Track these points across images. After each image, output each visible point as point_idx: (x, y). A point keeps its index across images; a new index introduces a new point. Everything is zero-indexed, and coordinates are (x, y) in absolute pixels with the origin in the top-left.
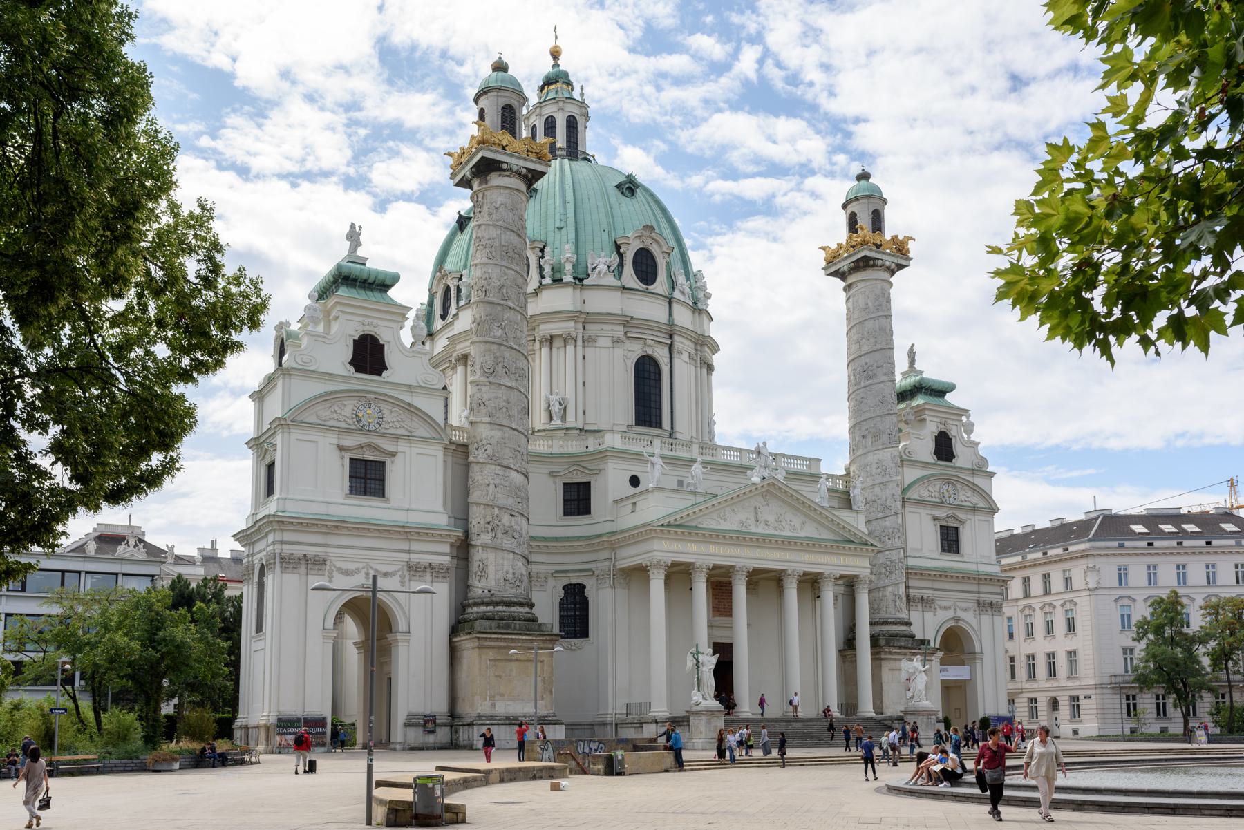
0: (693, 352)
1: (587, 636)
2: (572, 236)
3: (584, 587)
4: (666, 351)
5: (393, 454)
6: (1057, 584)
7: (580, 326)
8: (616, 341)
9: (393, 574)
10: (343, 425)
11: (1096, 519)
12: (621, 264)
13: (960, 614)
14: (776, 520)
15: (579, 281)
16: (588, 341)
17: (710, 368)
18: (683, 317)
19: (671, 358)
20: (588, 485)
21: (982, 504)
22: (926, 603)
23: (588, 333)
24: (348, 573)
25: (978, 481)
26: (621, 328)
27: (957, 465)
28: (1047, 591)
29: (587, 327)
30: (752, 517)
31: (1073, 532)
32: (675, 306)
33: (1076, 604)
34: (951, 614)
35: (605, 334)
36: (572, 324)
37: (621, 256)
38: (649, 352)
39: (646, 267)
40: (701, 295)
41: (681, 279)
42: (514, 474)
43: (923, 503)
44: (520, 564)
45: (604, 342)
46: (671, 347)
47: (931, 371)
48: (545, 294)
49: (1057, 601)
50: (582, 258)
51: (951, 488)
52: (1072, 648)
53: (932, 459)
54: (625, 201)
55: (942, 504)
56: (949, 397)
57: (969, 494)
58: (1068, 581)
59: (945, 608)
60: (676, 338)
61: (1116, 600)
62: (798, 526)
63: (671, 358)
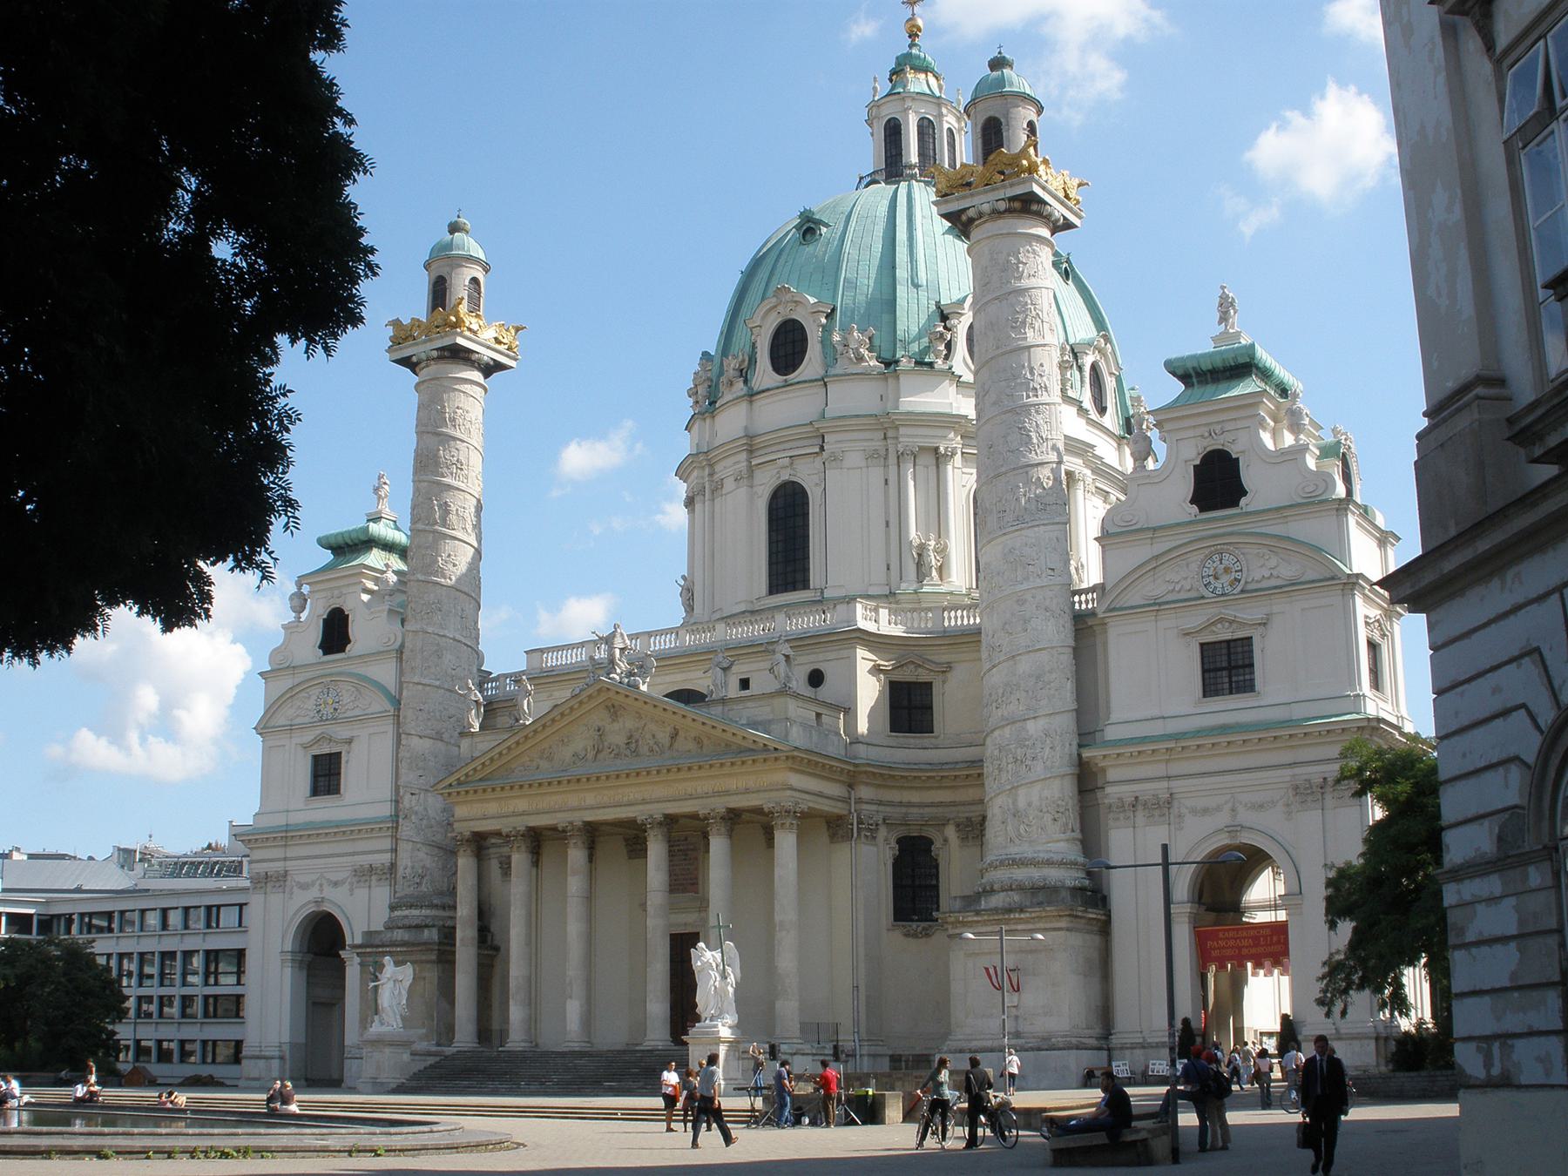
0: (878, 444)
5: (350, 741)
9: (343, 882)
10: (306, 720)
12: (752, 360)
13: (1245, 817)
16: (717, 488)
22: (1163, 807)
24: (304, 887)
26: (744, 456)
27: (1250, 509)
29: (718, 468)
34: (1223, 819)
36: (695, 473)
37: (754, 346)
38: (785, 477)
39: (788, 346)
42: (415, 741)
43: (1157, 606)
44: (421, 855)
45: (729, 484)
57: (1273, 562)
59: (1205, 811)
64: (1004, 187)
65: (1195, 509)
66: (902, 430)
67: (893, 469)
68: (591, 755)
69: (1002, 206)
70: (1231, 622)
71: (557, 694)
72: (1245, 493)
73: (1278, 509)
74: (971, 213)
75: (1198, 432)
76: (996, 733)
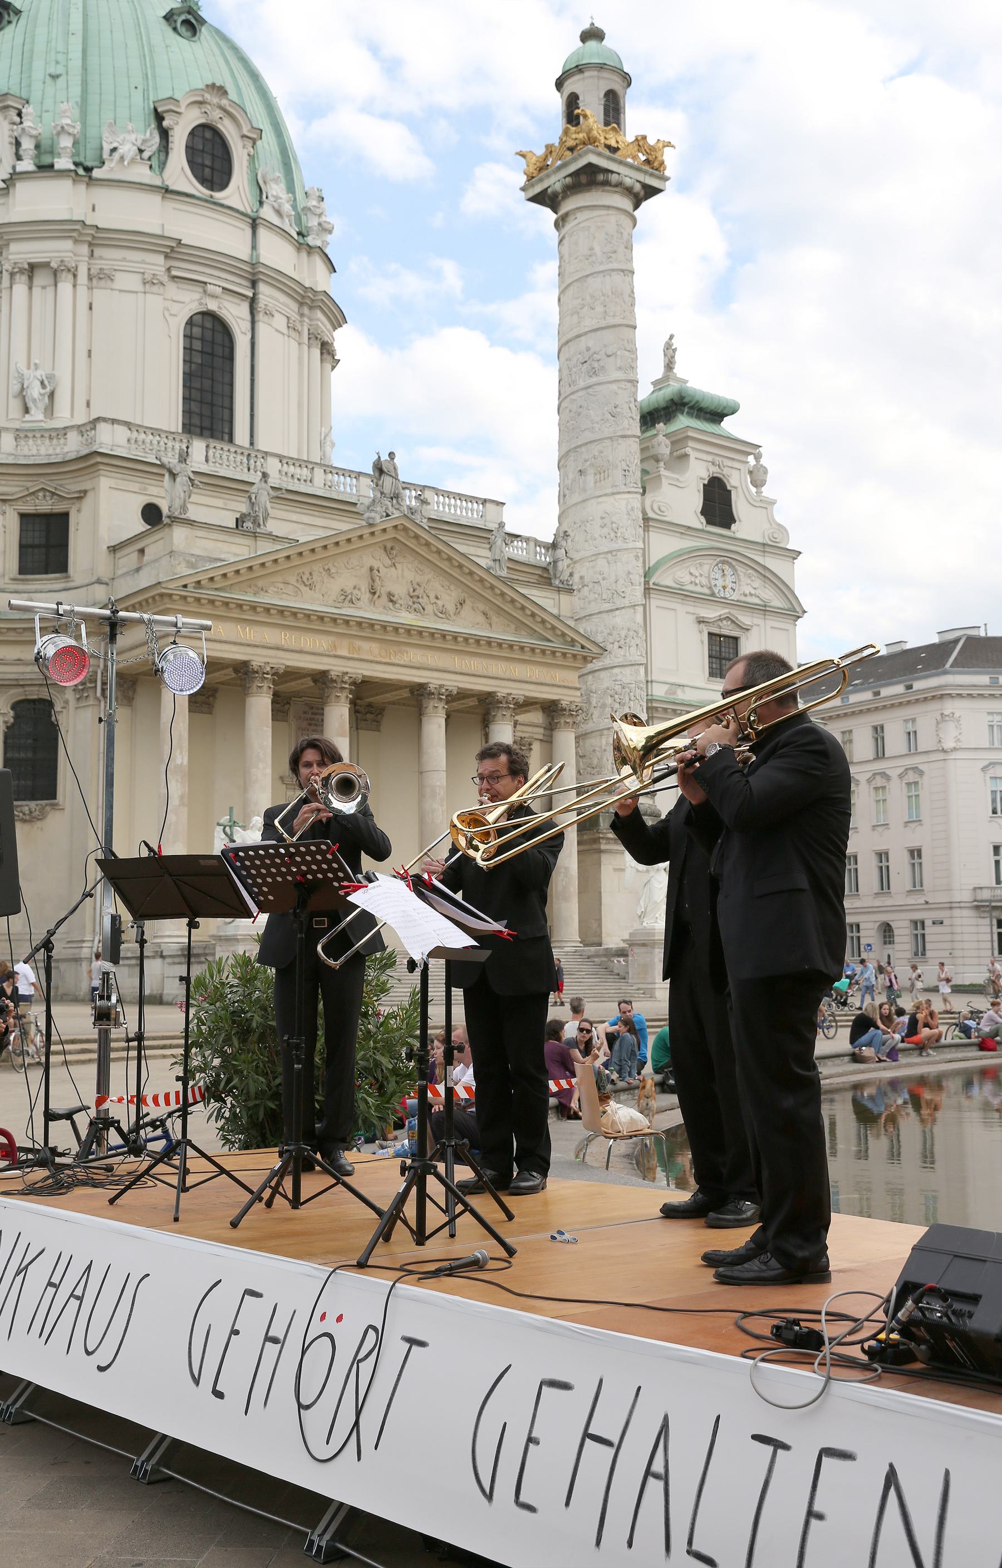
0: (294, 316)
1: (55, 798)
2: (76, 91)
3: (50, 704)
4: (244, 308)
6: (895, 742)
7: (85, 249)
8: (150, 282)
11: (956, 641)
14: (407, 592)
15: (84, 172)
16: (99, 277)
17: (327, 349)
18: (276, 253)
19: (253, 322)
20: (65, 516)
21: (777, 602)
23: (97, 265)
25: (773, 563)
26: (160, 259)
27: (738, 535)
28: (880, 754)
29: (98, 252)
30: (364, 586)
31: (921, 661)
32: (262, 232)
33: (921, 773)
35: (131, 267)
36: (68, 244)
37: (165, 134)
38: (212, 306)
39: (211, 159)
40: (313, 222)
41: (276, 190)
46: (253, 301)
47: (700, 378)
48: (22, 189)
49: (893, 768)
50: (92, 132)
51: (728, 571)
52: (915, 844)
53: (698, 521)
54: (180, 45)
55: (711, 598)
56: (728, 424)
57: (758, 583)
58: (911, 736)
60: (262, 287)
61: (984, 769)
62: (451, 608)
63: (253, 322)
64: (646, 172)
65: (703, 519)
66: (319, 314)
67: (306, 348)
68: (366, 596)
69: (638, 187)
70: (733, 622)
71: (154, 490)
72: (735, 521)
73: (764, 545)
74: (614, 178)
75: (710, 458)
76: (616, 671)
